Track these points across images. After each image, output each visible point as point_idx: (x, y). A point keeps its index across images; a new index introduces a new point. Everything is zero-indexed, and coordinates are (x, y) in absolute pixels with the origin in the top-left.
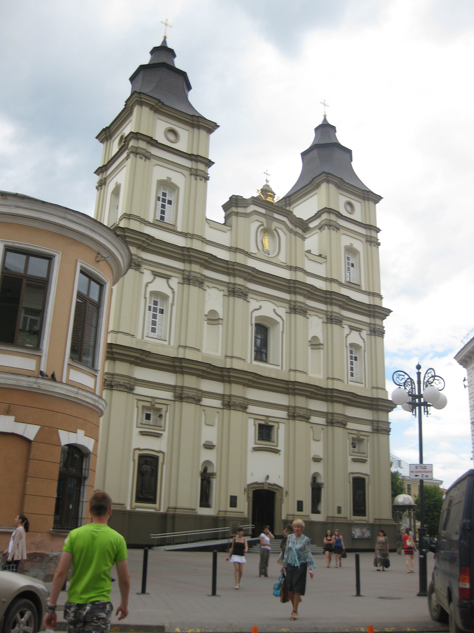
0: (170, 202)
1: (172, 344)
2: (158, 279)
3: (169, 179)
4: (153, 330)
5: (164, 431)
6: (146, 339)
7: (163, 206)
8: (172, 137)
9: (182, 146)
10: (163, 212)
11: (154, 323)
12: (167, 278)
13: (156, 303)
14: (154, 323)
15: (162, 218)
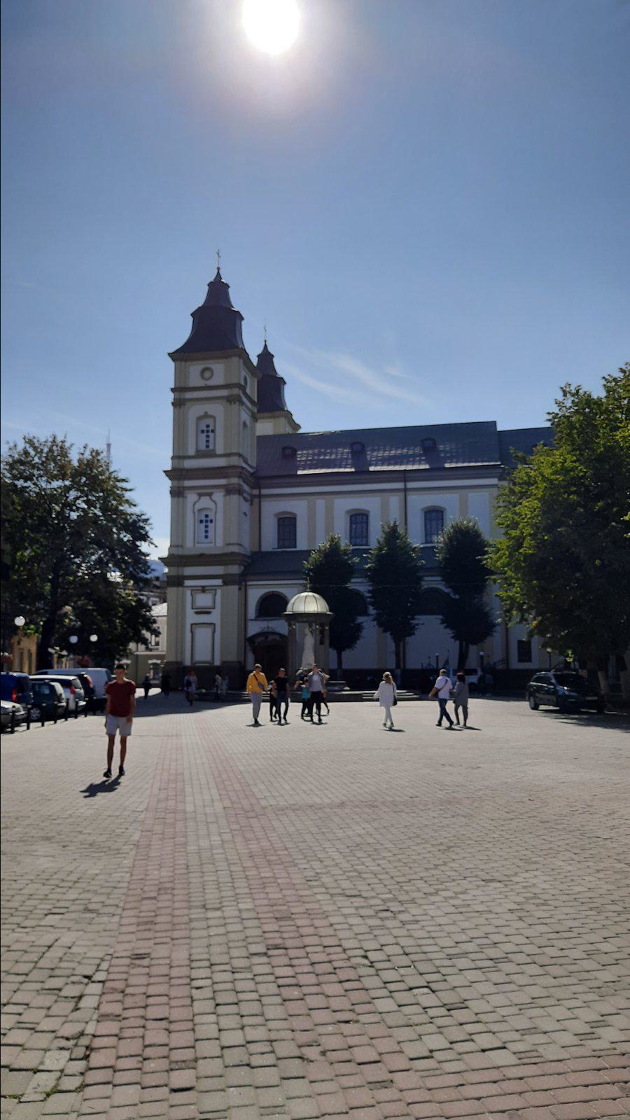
0: (213, 431)
1: (218, 545)
2: (202, 498)
3: (206, 413)
4: (206, 537)
5: (214, 608)
6: (197, 545)
7: (208, 436)
8: (207, 374)
9: (218, 379)
10: (207, 441)
11: (206, 532)
12: (210, 495)
13: (207, 516)
14: (206, 532)
15: (207, 446)
